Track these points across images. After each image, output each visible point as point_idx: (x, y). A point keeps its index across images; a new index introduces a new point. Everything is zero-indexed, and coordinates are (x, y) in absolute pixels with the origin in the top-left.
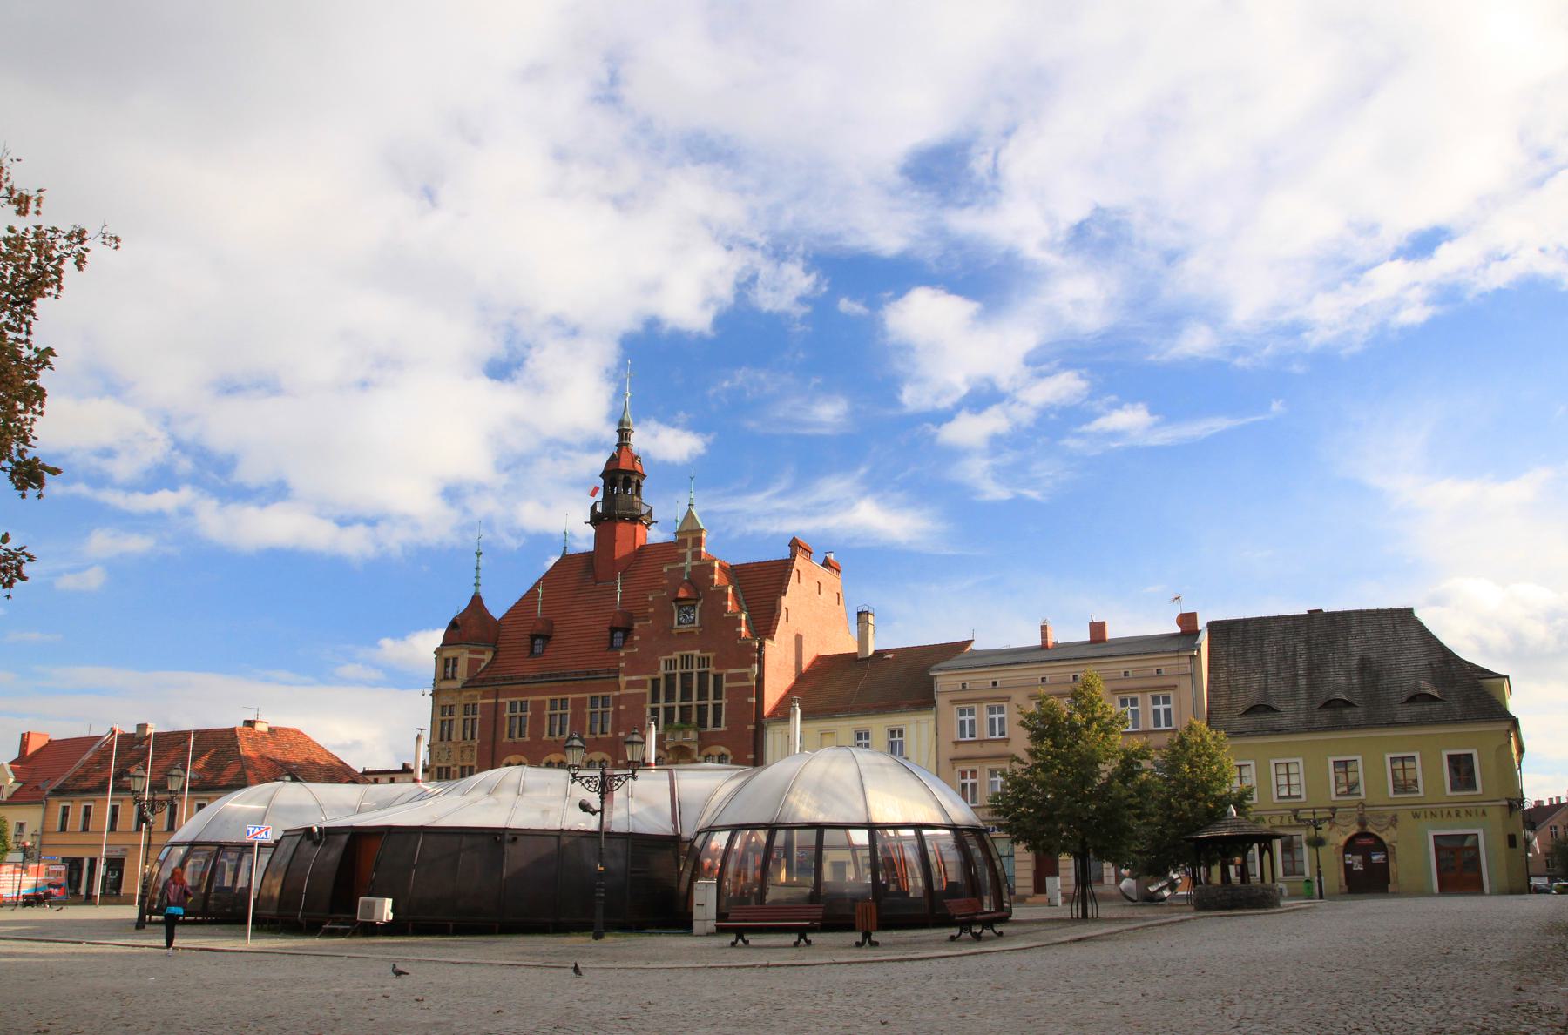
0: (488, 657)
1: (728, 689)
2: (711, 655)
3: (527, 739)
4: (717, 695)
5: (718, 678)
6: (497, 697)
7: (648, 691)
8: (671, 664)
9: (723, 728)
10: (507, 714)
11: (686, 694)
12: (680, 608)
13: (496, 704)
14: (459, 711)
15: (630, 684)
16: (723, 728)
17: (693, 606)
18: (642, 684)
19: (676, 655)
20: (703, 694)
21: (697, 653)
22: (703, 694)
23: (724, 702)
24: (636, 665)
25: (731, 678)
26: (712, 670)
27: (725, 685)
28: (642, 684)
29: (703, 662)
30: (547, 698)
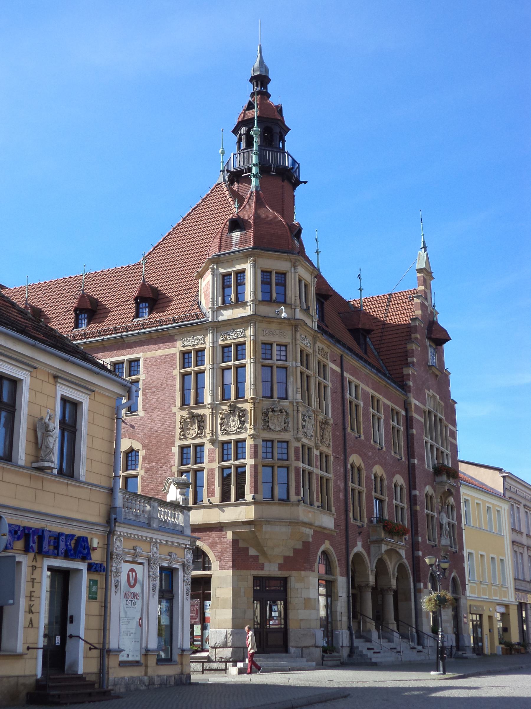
12: (430, 346)
21: (438, 398)
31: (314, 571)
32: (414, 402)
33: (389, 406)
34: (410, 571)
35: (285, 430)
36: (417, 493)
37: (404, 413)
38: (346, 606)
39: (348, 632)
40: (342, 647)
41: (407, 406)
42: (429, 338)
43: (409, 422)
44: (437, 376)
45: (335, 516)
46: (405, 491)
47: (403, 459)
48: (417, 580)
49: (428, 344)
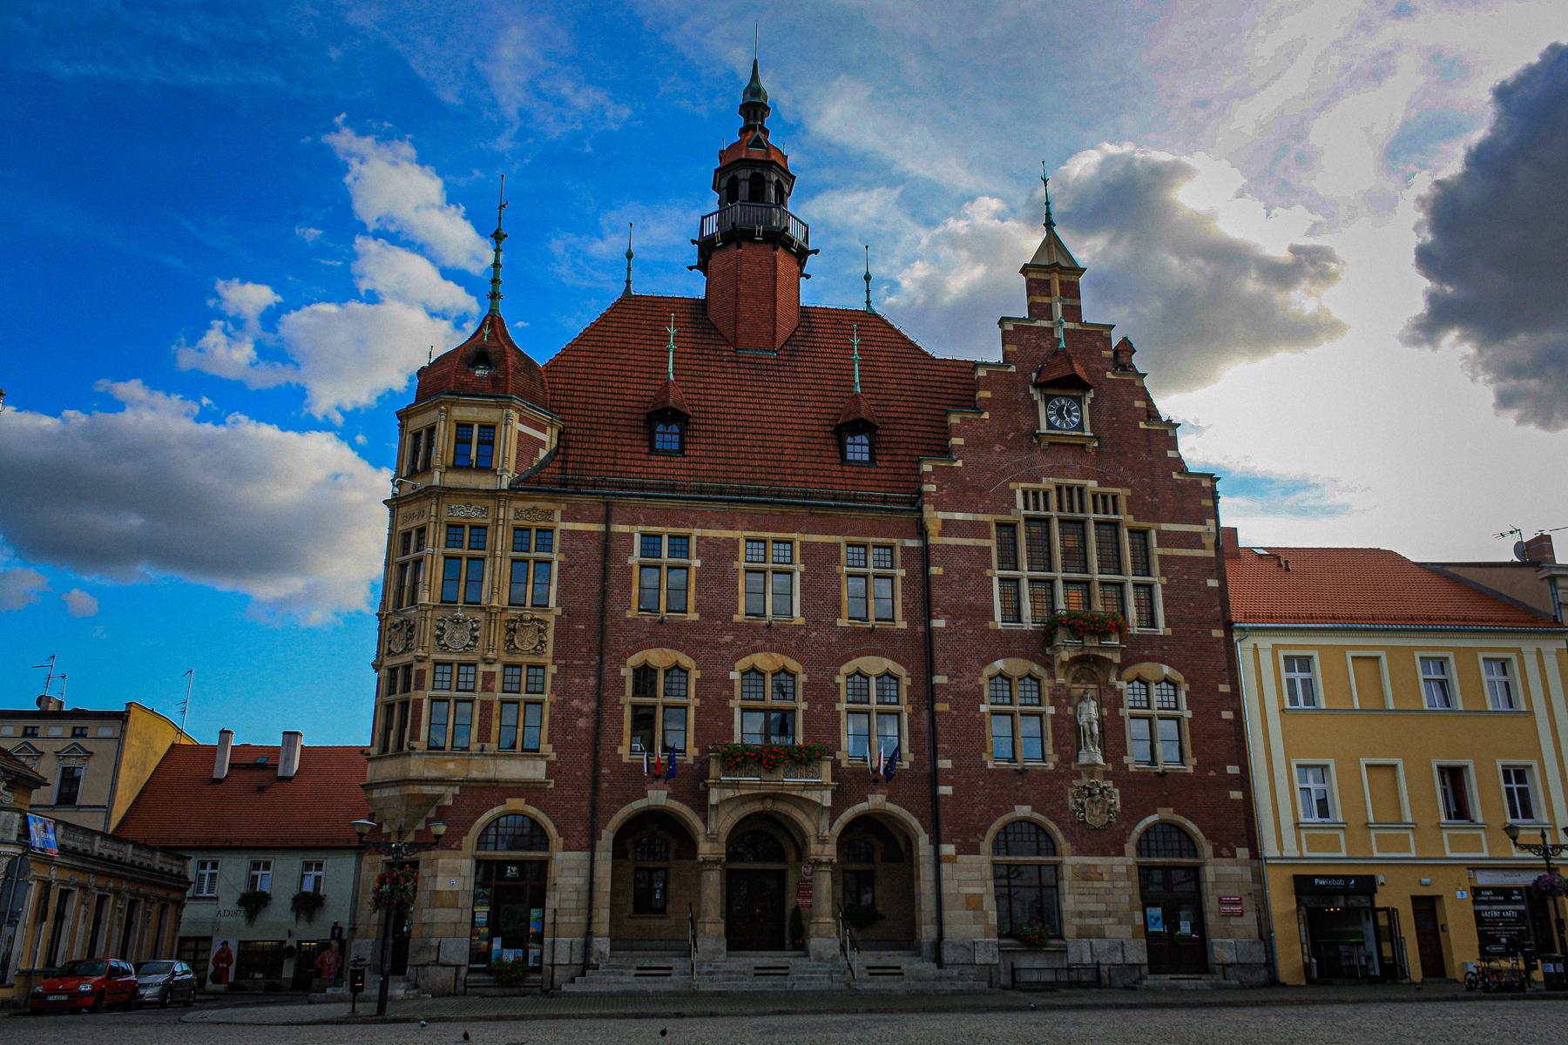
0: (548, 438)
1: (1162, 558)
2: (1123, 493)
3: (693, 616)
4: (1143, 566)
5: (1140, 535)
6: (607, 521)
7: (991, 543)
8: (1033, 497)
9: (1162, 628)
10: (635, 559)
11: (1077, 557)
12: (1048, 399)
13: (607, 536)
14: (501, 540)
15: (948, 528)
16: (1162, 628)
17: (1079, 401)
18: (978, 529)
19: (1048, 483)
20: (1112, 561)
21: (1092, 484)
22: (1112, 561)
23: (1158, 580)
24: (960, 493)
25: (1165, 539)
26: (1126, 518)
27: (1156, 551)
28: (978, 529)
29: (1102, 502)
30: (739, 534)
31: (459, 848)
32: (934, 517)
33: (837, 545)
34: (915, 823)
35: (407, 649)
36: (940, 679)
37: (912, 543)
38: (584, 896)
39: (580, 940)
40: (553, 965)
41: (921, 531)
42: (1036, 386)
43: (925, 555)
44: (1083, 446)
45: (553, 757)
46: (906, 681)
47: (902, 624)
48: (936, 842)
49: (1037, 396)
